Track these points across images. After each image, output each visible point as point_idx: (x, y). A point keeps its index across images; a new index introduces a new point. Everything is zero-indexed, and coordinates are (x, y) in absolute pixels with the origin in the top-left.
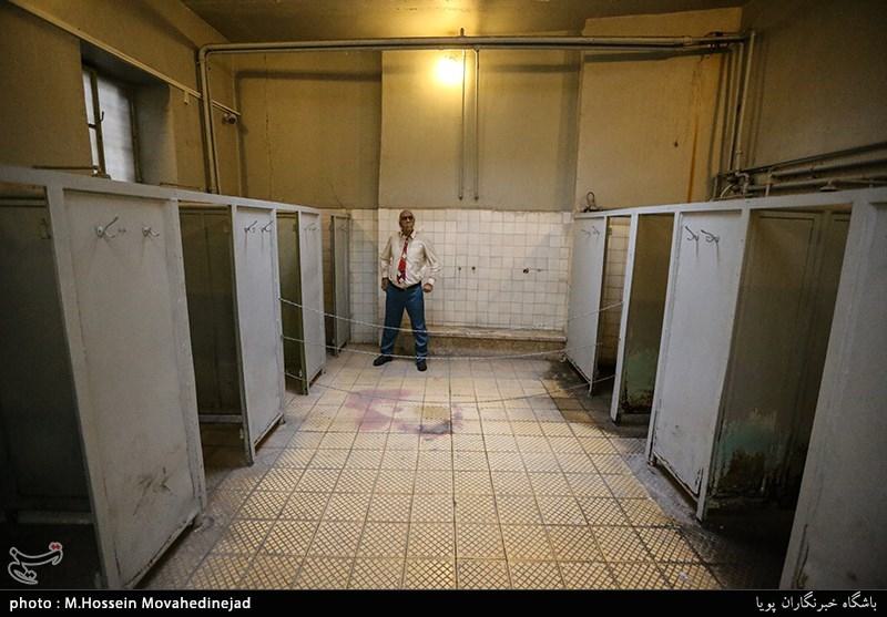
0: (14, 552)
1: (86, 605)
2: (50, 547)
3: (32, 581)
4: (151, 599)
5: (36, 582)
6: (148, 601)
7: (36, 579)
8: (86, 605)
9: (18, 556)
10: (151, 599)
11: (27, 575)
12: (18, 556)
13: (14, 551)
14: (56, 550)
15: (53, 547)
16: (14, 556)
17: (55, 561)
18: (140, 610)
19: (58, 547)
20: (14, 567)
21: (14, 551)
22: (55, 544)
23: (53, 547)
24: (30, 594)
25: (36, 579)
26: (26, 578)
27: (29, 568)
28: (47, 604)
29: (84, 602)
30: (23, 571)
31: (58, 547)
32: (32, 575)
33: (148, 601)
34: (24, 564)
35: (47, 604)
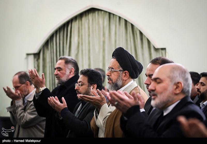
0: (3, 129)
1: (15, 141)
2: (11, 128)
3: (7, 136)
4: (28, 140)
5: (8, 136)
6: (27, 140)
8: (15, 141)
9: (4, 130)
10: (28, 140)
11: (6, 134)
12: (4, 130)
13: (3, 129)
14: (13, 128)
15: (12, 128)
16: (3, 130)
17: (13, 131)
18: (25, 142)
19: (13, 128)
20: (3, 132)
21: (3, 129)
22: (13, 127)
23: (12, 128)
24: (6, 138)
27: (7, 133)
28: (10, 141)
29: (14, 141)
30: (5, 133)
31: (13, 128)
32: (7, 134)
33: (27, 140)
34: (4, 131)
35: (10, 141)
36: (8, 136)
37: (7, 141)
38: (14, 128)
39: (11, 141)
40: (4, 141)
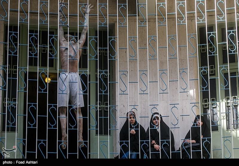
0: (3, 148)
2: (13, 147)
5: (10, 157)
7: (9, 156)
11: (7, 155)
14: (15, 148)
15: (14, 147)
19: (15, 147)
23: (14, 147)
25: (9, 156)
26: (7, 155)
28: (11, 162)
34: (6, 152)
35: (11, 162)
36: (10, 157)
37: (8, 162)
38: (16, 148)
39: (13, 163)
40: (4, 163)
